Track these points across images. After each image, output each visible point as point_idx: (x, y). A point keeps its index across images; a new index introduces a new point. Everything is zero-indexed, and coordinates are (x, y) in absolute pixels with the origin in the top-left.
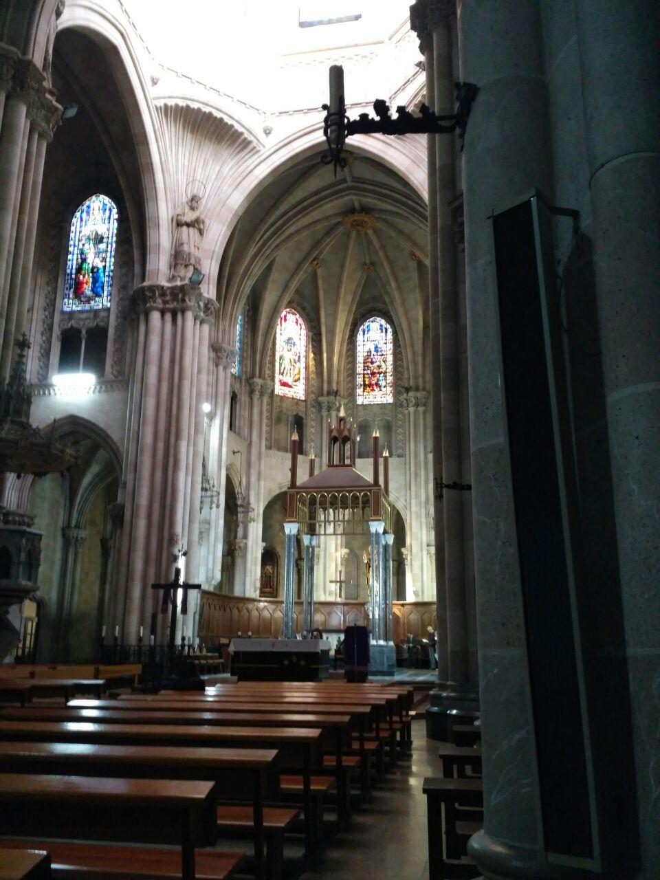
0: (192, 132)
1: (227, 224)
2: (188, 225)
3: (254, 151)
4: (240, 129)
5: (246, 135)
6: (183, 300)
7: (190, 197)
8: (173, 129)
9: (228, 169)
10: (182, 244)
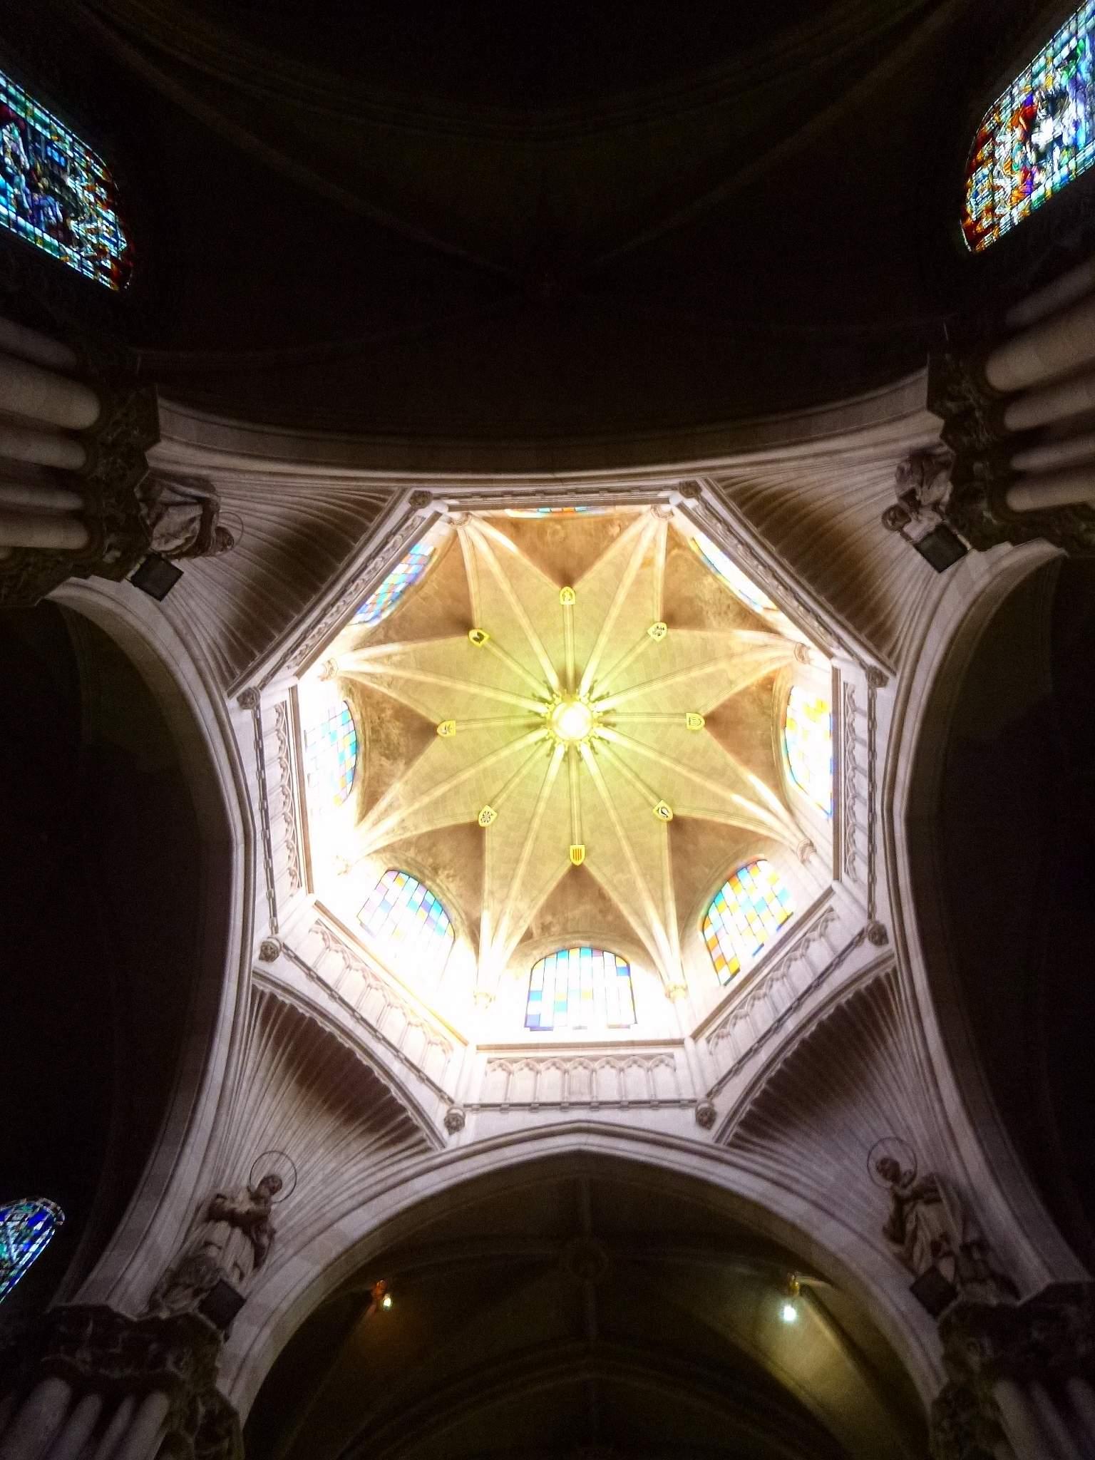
0: (300, 1082)
1: (324, 1263)
2: (234, 1219)
3: (422, 1147)
4: (402, 1101)
5: (410, 1112)
6: (159, 1361)
7: (256, 1184)
8: (268, 1053)
9: (354, 1170)
10: (208, 1244)
